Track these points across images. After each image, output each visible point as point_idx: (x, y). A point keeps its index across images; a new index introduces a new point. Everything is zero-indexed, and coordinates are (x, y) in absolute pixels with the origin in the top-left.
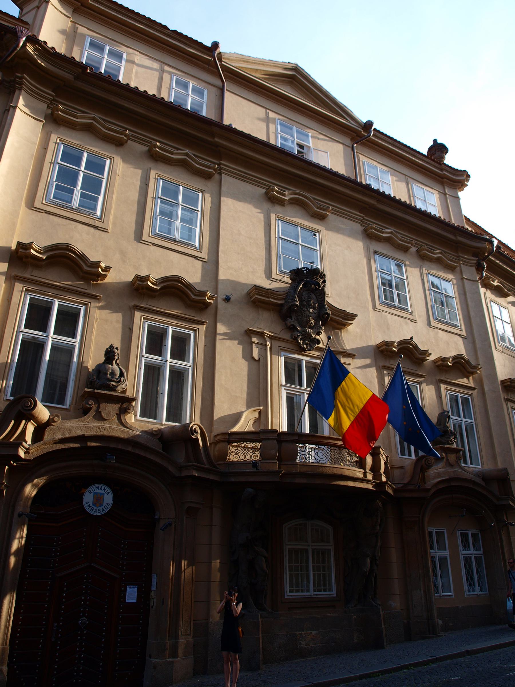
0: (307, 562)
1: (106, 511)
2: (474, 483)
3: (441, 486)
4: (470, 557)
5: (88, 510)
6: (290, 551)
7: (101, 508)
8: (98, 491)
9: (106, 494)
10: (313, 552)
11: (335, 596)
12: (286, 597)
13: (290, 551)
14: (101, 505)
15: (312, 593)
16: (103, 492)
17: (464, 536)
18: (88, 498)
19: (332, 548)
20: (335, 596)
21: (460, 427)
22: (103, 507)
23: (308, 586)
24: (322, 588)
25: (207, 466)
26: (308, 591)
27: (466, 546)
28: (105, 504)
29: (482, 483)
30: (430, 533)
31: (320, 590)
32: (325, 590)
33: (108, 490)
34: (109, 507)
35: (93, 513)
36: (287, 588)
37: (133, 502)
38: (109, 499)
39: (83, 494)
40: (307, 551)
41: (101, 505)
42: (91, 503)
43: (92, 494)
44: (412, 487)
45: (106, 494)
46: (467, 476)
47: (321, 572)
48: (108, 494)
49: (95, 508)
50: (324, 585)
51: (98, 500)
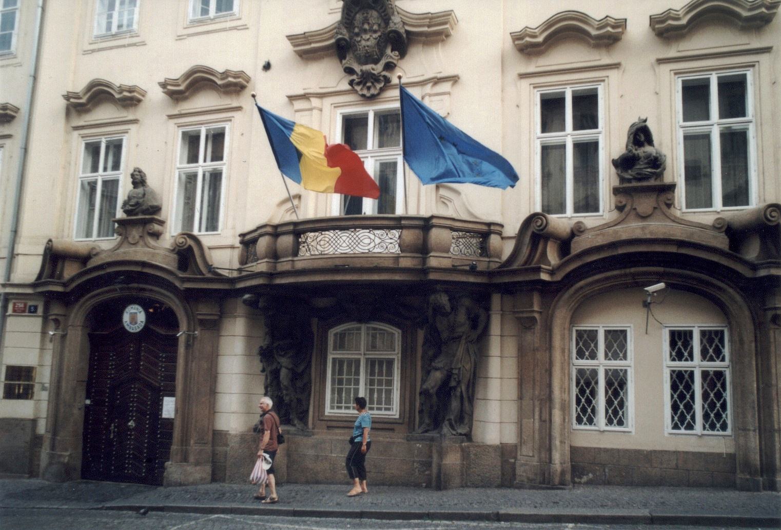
1: (141, 328)
7: (136, 326)
8: (133, 311)
9: (138, 313)
13: (334, 359)
14: (136, 323)
18: (126, 318)
19: (396, 356)
28: (139, 322)
34: (143, 324)
37: (161, 318)
38: (141, 317)
40: (358, 362)
41: (136, 323)
42: (128, 322)
46: (678, 232)
48: (140, 312)
50: (379, 402)
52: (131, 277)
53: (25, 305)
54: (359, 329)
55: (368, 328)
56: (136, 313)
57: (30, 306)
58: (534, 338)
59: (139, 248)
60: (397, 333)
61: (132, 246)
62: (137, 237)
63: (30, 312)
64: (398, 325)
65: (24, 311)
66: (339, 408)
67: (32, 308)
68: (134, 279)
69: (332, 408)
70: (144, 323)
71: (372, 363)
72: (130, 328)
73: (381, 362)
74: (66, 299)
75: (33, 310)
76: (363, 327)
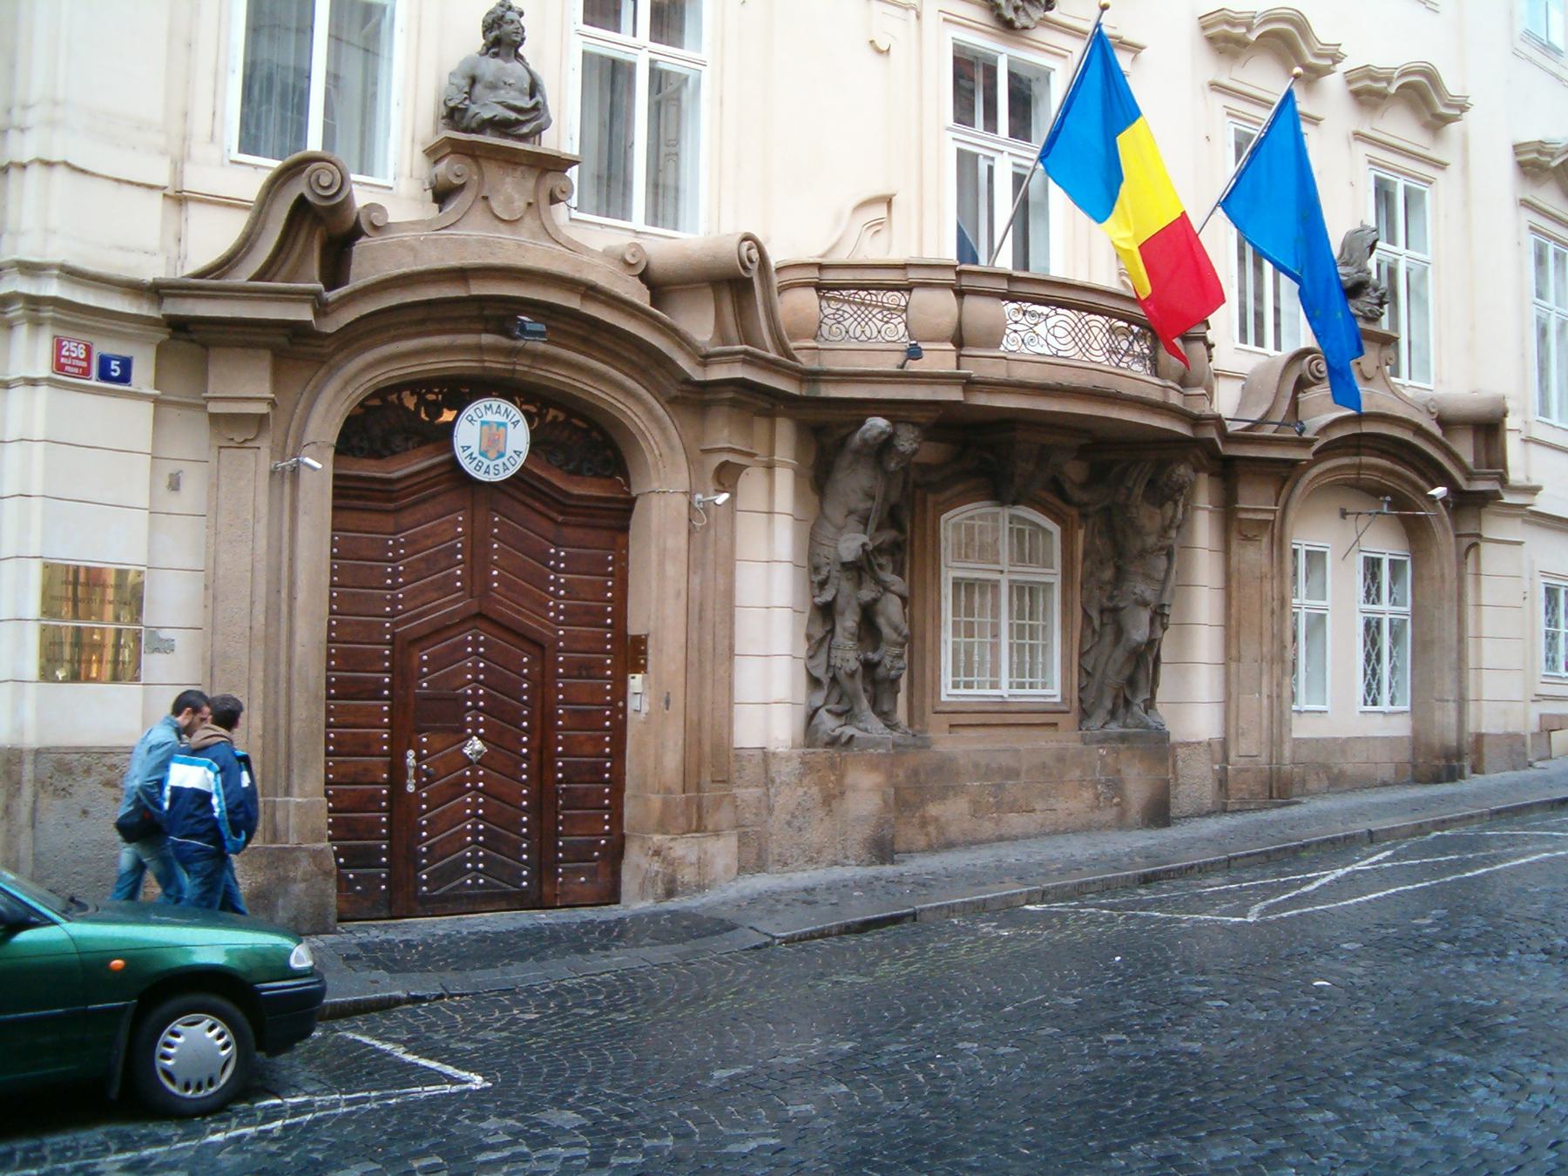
0: (996, 613)
1: (513, 470)
2: (1418, 430)
3: (1337, 434)
4: (1379, 622)
5: (468, 467)
6: (957, 584)
7: (499, 462)
8: (490, 417)
9: (510, 426)
10: (1011, 587)
11: (1058, 699)
12: (944, 698)
15: (1004, 690)
16: (503, 419)
17: (1372, 566)
19: (1057, 581)
20: (1058, 699)
21: (1392, 273)
22: (504, 459)
23: (995, 671)
24: (1027, 679)
25: (773, 355)
26: (994, 685)
27: (1373, 594)
28: (509, 453)
29: (1436, 431)
30: (1295, 552)
31: (1021, 686)
32: (1031, 687)
33: (516, 414)
34: (521, 461)
35: (480, 476)
36: (947, 678)
38: (518, 438)
39: (451, 426)
40: (995, 585)
41: (501, 455)
42: (475, 450)
43: (478, 424)
44: (1268, 431)
45: (510, 426)
47: (1027, 641)
48: (515, 424)
49: (486, 462)
51: (493, 442)
52: (499, 316)
53: (88, 350)
54: (995, 518)
55: (1012, 518)
56: (504, 425)
57: (105, 362)
58: (1253, 556)
59: (523, 235)
60: (1055, 529)
61: (502, 225)
62: (520, 204)
63: (105, 375)
64: (1058, 518)
65: (86, 373)
66: (968, 685)
67: (114, 364)
68: (505, 324)
69: (956, 685)
70: (524, 456)
71: (1018, 589)
72: (478, 467)
73: (1021, 589)
74: (295, 350)
75: (115, 373)
76: (1006, 512)
